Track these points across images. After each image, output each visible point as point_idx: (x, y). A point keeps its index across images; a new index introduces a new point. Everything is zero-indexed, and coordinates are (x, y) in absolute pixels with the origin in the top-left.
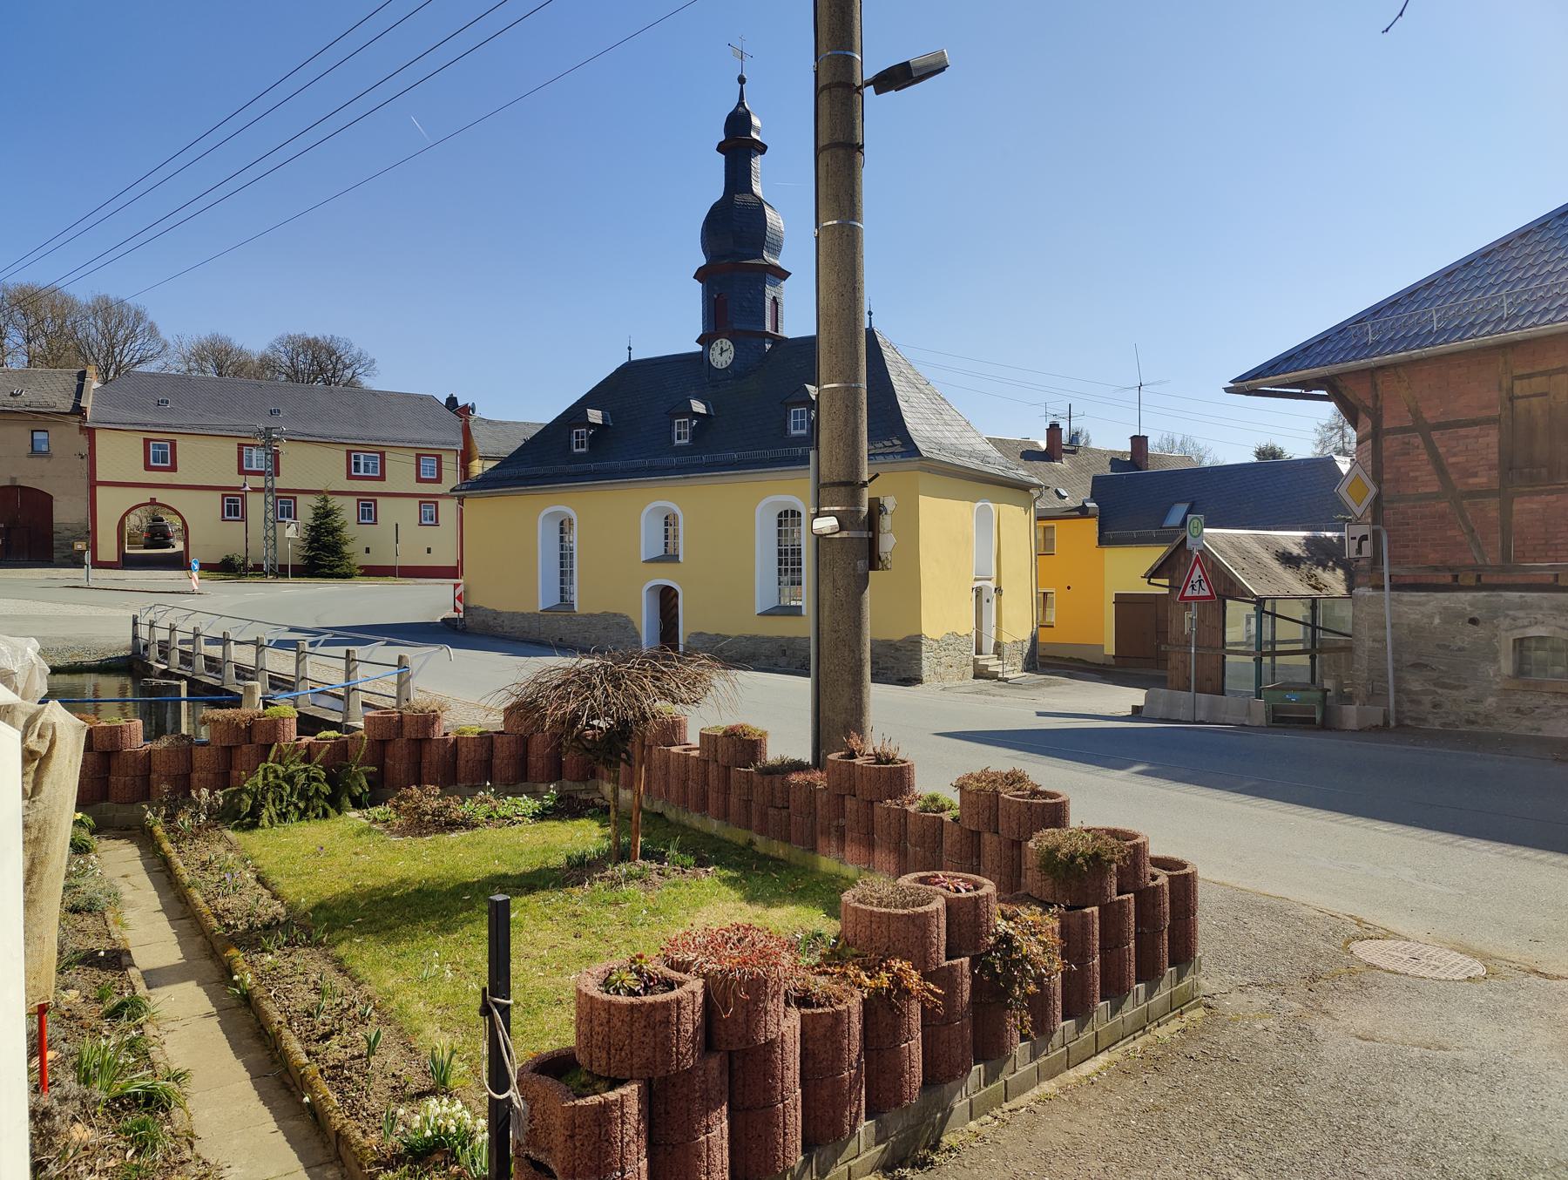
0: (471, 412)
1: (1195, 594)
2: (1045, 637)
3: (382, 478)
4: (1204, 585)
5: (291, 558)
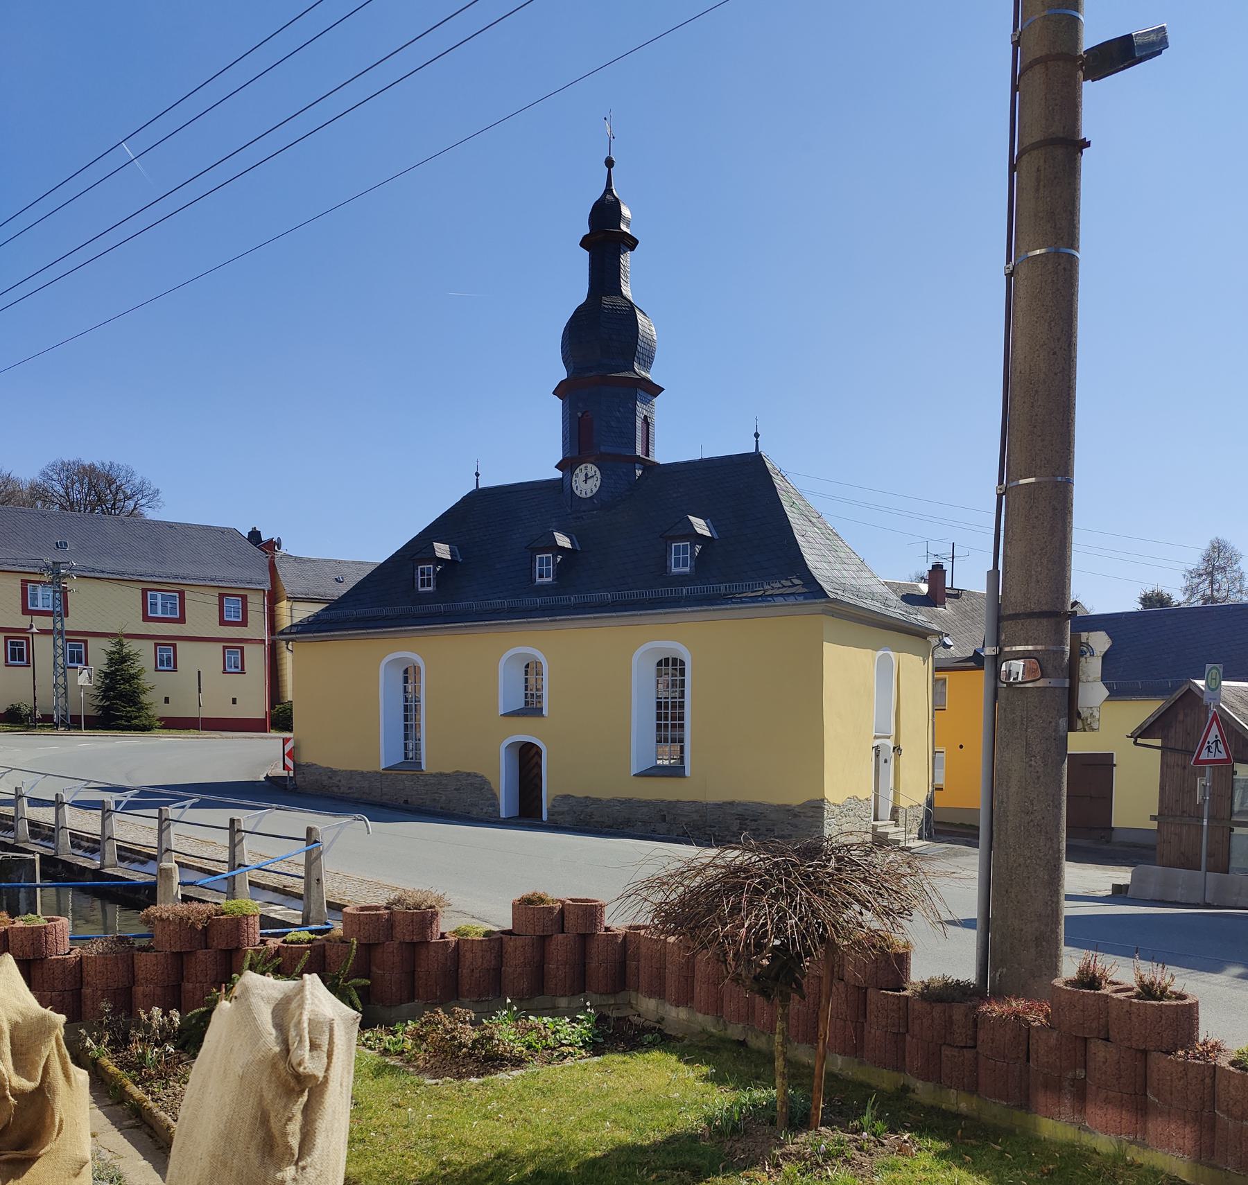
0: (276, 548)
1: (1211, 757)
2: (940, 801)
3: (182, 620)
4: (1221, 747)
5: (84, 706)
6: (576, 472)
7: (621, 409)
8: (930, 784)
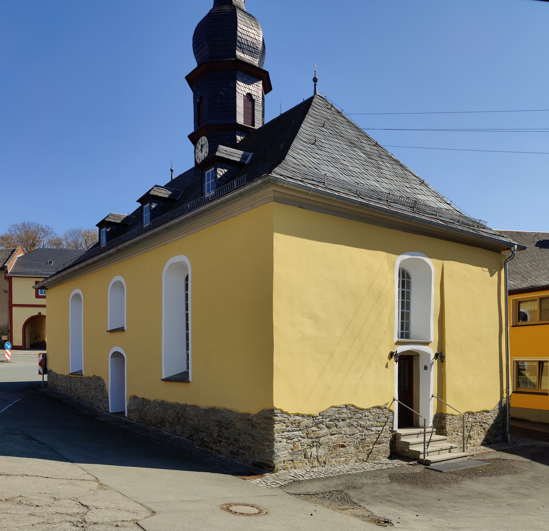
6: (197, 146)
7: (224, 89)
8: (505, 391)
